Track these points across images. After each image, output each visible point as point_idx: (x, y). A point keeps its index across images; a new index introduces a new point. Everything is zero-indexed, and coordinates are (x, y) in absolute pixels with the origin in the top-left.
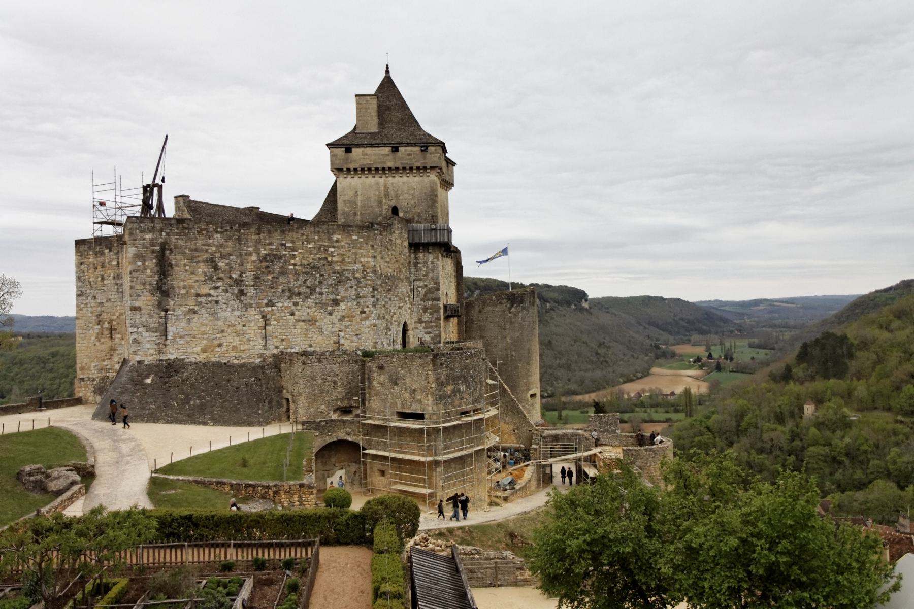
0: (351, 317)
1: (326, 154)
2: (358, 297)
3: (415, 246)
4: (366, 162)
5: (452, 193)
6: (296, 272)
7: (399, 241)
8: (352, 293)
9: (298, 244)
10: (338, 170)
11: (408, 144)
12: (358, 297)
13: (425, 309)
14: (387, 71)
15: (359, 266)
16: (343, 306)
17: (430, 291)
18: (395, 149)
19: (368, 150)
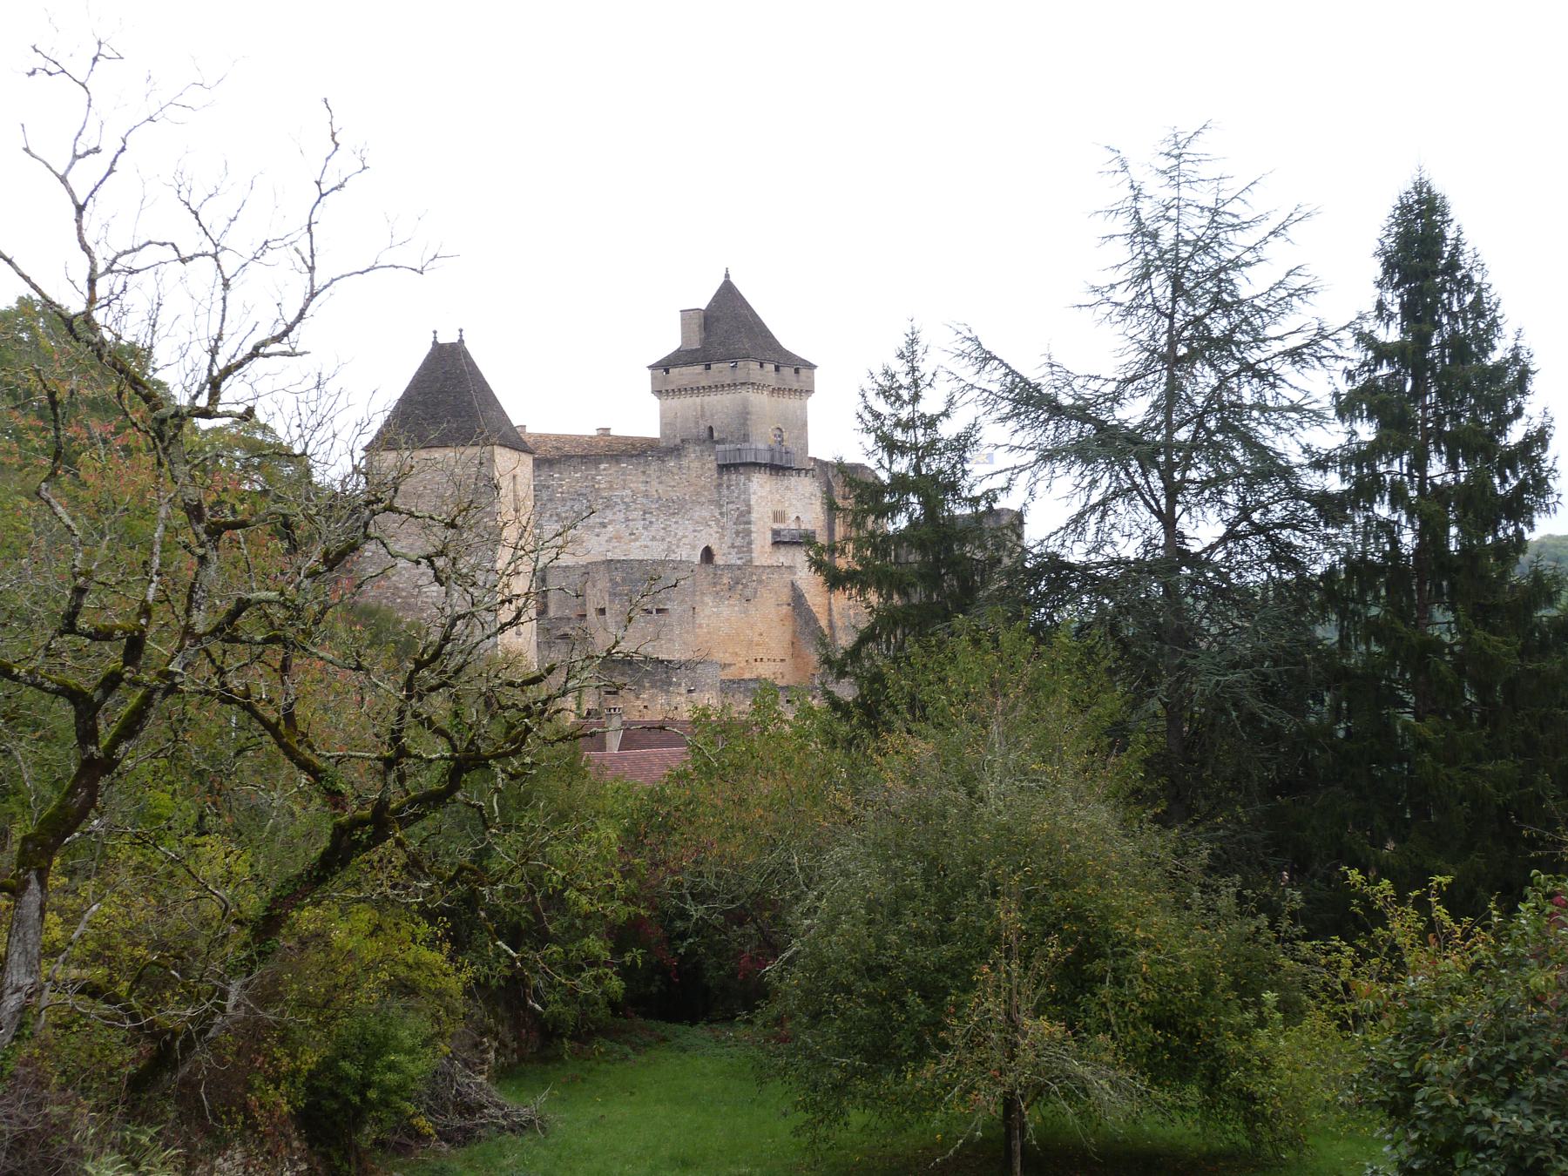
0: (619, 538)
1: (647, 375)
2: (627, 520)
3: (724, 468)
4: (684, 382)
5: (812, 403)
6: (563, 499)
7: (696, 464)
8: (621, 516)
9: (565, 475)
10: (658, 392)
11: (719, 361)
12: (627, 520)
13: (737, 533)
14: (727, 276)
15: (629, 492)
16: (610, 528)
17: (742, 514)
18: (708, 367)
19: (684, 370)
